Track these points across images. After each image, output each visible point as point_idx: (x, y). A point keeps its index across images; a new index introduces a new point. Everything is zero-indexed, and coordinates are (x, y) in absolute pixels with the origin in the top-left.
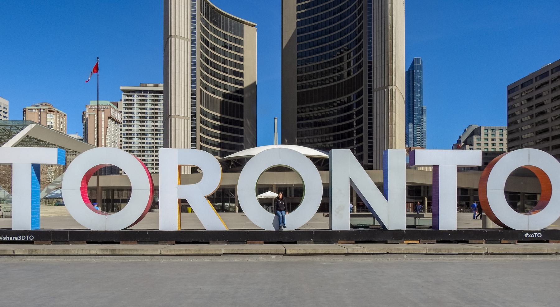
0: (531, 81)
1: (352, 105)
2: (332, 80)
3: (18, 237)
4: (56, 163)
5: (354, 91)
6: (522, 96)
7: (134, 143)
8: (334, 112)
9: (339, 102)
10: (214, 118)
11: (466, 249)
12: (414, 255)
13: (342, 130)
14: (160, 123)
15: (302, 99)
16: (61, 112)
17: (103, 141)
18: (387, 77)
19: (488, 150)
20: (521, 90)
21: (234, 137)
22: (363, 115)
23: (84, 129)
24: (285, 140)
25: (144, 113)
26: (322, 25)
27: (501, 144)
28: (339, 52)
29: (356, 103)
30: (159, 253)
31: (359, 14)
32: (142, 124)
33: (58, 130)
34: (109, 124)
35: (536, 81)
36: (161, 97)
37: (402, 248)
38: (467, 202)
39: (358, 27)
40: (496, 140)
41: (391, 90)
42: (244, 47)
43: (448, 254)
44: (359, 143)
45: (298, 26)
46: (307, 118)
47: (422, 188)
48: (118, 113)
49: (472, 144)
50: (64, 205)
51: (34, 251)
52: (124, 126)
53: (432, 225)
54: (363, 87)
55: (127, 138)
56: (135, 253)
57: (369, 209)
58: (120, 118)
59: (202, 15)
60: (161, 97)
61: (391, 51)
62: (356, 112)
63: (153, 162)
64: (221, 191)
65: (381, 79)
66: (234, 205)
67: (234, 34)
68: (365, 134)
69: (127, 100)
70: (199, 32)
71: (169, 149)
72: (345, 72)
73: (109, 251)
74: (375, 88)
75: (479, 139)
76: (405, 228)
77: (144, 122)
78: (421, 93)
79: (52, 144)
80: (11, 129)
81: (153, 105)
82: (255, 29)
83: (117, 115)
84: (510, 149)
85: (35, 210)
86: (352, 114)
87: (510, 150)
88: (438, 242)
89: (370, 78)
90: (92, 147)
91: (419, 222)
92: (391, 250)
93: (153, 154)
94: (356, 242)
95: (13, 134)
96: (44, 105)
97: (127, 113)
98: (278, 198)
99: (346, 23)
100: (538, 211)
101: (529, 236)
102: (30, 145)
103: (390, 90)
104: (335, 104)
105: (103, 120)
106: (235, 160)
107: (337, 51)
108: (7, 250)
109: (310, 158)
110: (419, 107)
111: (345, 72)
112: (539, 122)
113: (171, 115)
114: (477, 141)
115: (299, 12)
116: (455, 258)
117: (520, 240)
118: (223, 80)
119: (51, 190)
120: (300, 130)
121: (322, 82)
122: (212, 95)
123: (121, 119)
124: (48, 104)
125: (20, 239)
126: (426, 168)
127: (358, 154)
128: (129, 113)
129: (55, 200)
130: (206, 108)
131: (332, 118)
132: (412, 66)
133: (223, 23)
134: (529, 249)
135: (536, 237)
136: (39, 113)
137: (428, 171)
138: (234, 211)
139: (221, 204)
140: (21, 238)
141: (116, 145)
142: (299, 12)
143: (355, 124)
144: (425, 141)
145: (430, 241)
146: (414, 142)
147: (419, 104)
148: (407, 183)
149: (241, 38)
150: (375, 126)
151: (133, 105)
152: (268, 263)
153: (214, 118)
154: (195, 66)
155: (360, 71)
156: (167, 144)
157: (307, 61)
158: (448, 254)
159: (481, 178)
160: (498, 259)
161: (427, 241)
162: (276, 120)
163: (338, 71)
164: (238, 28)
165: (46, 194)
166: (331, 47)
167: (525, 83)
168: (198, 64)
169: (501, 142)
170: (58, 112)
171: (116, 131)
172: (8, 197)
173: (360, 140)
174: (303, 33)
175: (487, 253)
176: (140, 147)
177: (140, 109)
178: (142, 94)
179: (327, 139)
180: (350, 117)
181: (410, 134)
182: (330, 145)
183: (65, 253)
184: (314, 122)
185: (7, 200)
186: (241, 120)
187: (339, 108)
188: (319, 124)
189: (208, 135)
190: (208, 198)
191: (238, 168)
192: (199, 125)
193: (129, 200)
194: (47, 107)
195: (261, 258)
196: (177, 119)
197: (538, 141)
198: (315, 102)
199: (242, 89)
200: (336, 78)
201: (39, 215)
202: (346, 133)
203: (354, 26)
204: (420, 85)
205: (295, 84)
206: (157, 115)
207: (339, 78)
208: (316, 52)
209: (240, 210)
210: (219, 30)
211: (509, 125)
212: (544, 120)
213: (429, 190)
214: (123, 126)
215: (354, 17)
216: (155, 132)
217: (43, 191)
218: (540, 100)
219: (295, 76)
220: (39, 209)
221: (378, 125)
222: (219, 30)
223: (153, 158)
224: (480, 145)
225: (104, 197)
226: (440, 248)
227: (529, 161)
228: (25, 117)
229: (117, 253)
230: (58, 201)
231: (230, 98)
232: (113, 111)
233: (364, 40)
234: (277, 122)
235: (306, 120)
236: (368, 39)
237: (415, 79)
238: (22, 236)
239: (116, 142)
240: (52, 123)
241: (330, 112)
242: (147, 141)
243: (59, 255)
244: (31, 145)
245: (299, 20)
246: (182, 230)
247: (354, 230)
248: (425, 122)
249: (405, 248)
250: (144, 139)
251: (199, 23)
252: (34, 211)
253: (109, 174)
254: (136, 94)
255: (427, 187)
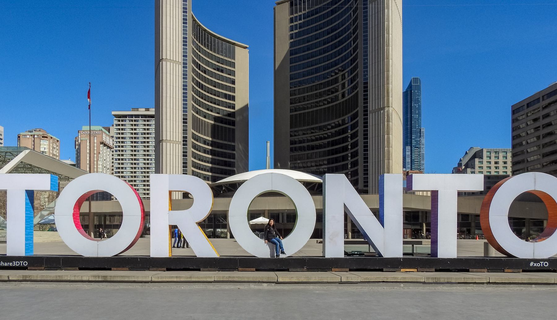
0: (538, 100)
1: (347, 127)
2: (326, 102)
3: (13, 263)
4: (49, 188)
5: (349, 113)
6: (527, 116)
7: (126, 168)
8: (328, 135)
9: (333, 125)
10: (205, 142)
11: (466, 278)
12: (412, 284)
13: (336, 153)
14: (151, 147)
15: (295, 121)
16: (54, 137)
17: (95, 166)
18: (384, 98)
19: (490, 174)
20: (526, 111)
21: (225, 162)
22: (358, 138)
23: (77, 154)
24: (278, 165)
25: (135, 138)
26: (316, 45)
27: (504, 167)
28: (333, 73)
29: (351, 125)
30: (149, 279)
31: (354, 33)
32: (134, 149)
33: (51, 155)
34: (101, 149)
35: (543, 100)
36: (153, 122)
37: (398, 276)
38: (468, 228)
39: (353, 47)
40: (500, 163)
41: (388, 111)
42: (236, 70)
43: (448, 283)
44: (354, 167)
45: (290, 47)
46: (300, 142)
47: (420, 214)
48: (109, 138)
50: (56, 231)
51: (28, 277)
52: (116, 151)
53: (430, 253)
54: (358, 108)
55: (119, 164)
56: (126, 279)
57: (365, 236)
58: (112, 143)
59: (193, 37)
60: (153, 122)
61: (388, 71)
62: (351, 135)
63: (144, 188)
64: (213, 216)
65: (377, 101)
66: (226, 230)
67: (226, 56)
68: (360, 158)
69: (119, 125)
70: (190, 55)
71: (161, 174)
72: (339, 93)
73: (100, 277)
74: (371, 109)
75: (482, 162)
76: (401, 256)
77: (135, 147)
78: (419, 114)
79: (45, 170)
80: (5, 155)
81: (145, 129)
82: (247, 50)
83: (109, 140)
84: (514, 173)
85: (28, 236)
86: (347, 137)
87: (515, 173)
88: (437, 271)
89: (366, 99)
90: (85, 173)
91: (416, 251)
92: (387, 279)
93: (144, 179)
94: (350, 270)
95: (8, 160)
96: (38, 131)
97: (119, 138)
98: (269, 224)
99: (341, 43)
100: (544, 238)
101: (535, 265)
102: (24, 171)
103: (387, 111)
104: (329, 127)
105: (95, 145)
106: (227, 185)
107: (331, 72)
108: (2, 276)
109: (303, 183)
110: (417, 129)
111: (339, 93)
112: (546, 144)
113: (162, 140)
115: (292, 32)
116: (455, 288)
117: (525, 269)
118: (215, 103)
119: (44, 216)
120: (293, 154)
121: (316, 104)
122: (204, 119)
123: (113, 144)
124: (42, 130)
125: (14, 264)
126: (425, 193)
127: (353, 179)
128: (121, 139)
129: (49, 226)
130: (197, 132)
131: (326, 141)
132: (410, 86)
133: (215, 45)
134: (534, 278)
135: (542, 266)
136: (33, 139)
137: (427, 196)
138: (226, 237)
139: (212, 230)
140: (16, 263)
141: (108, 170)
142: (292, 32)
143: (349, 147)
144: (423, 164)
145: (428, 270)
146: (411, 166)
147: (417, 126)
148: (404, 208)
149: (233, 61)
150: (371, 149)
151: (125, 130)
152: (259, 291)
153: (205, 142)
154: (186, 89)
155: (356, 92)
156: (158, 170)
157: (300, 83)
158: (448, 283)
159: (483, 204)
160: (501, 288)
161: (425, 270)
162: (269, 144)
163: (333, 93)
164: (230, 50)
165: (40, 219)
166: (325, 68)
167: (530, 103)
168: (189, 88)
169: (505, 165)
170: (51, 138)
171: (108, 157)
172: (4, 223)
173: (355, 164)
174: (296, 53)
175: (489, 283)
176: (132, 172)
177: (132, 134)
178: (134, 119)
179: (321, 163)
180: (345, 140)
181: (407, 157)
182: (324, 169)
183: (58, 279)
184: (307, 145)
185: (2, 226)
186: (233, 144)
187: (333, 131)
188: (313, 148)
189: (199, 160)
190: (201, 224)
191: (229, 193)
192: (190, 150)
193: (120, 225)
194: (41, 133)
195: (252, 286)
196: (168, 144)
197: (545, 164)
198: (308, 125)
199: (234, 113)
200: (329, 100)
201: (33, 241)
202: (341, 156)
203: (349, 45)
204: (419, 106)
205: (288, 106)
206: (148, 140)
207: (333, 100)
208: (309, 73)
209: (232, 237)
210: (210, 52)
211: (514, 147)
212: (551, 141)
213: (427, 215)
214: (114, 151)
215: (348, 37)
216: (147, 157)
217: (37, 217)
218: (547, 121)
219: (288, 99)
220: (33, 235)
221: (374, 148)
222: (210, 52)
223: (144, 183)
224: (482, 169)
225: (96, 223)
226: (439, 277)
227: (535, 185)
228: (20, 143)
229: (109, 279)
230: (50, 227)
231: (222, 122)
232: (105, 136)
233: (360, 60)
234: (269, 146)
235: (299, 143)
236: (363, 59)
237: (413, 99)
238: (17, 262)
239: (108, 167)
240: (46, 148)
241: (324, 135)
242: (138, 166)
243: (52, 281)
244: (25, 171)
245: (292, 40)
246: (173, 257)
247: (348, 257)
248: (423, 145)
249: (401, 277)
250: (135, 164)
251: (190, 45)
252: (29, 237)
253: (101, 199)
254: (128, 119)
255: (426, 213)
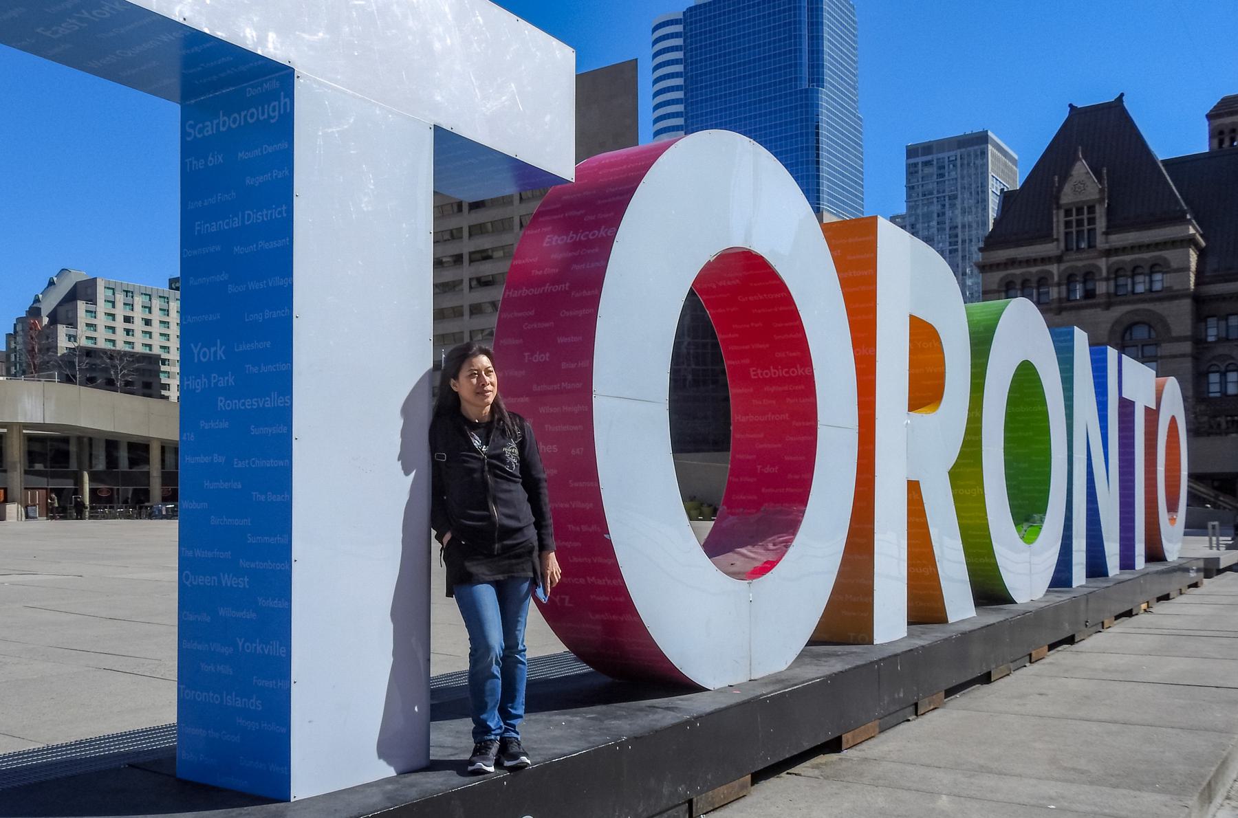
19: (150, 350)
49: (72, 323)
75: (93, 313)
114: (86, 316)
169: (148, 329)
224: (95, 331)
